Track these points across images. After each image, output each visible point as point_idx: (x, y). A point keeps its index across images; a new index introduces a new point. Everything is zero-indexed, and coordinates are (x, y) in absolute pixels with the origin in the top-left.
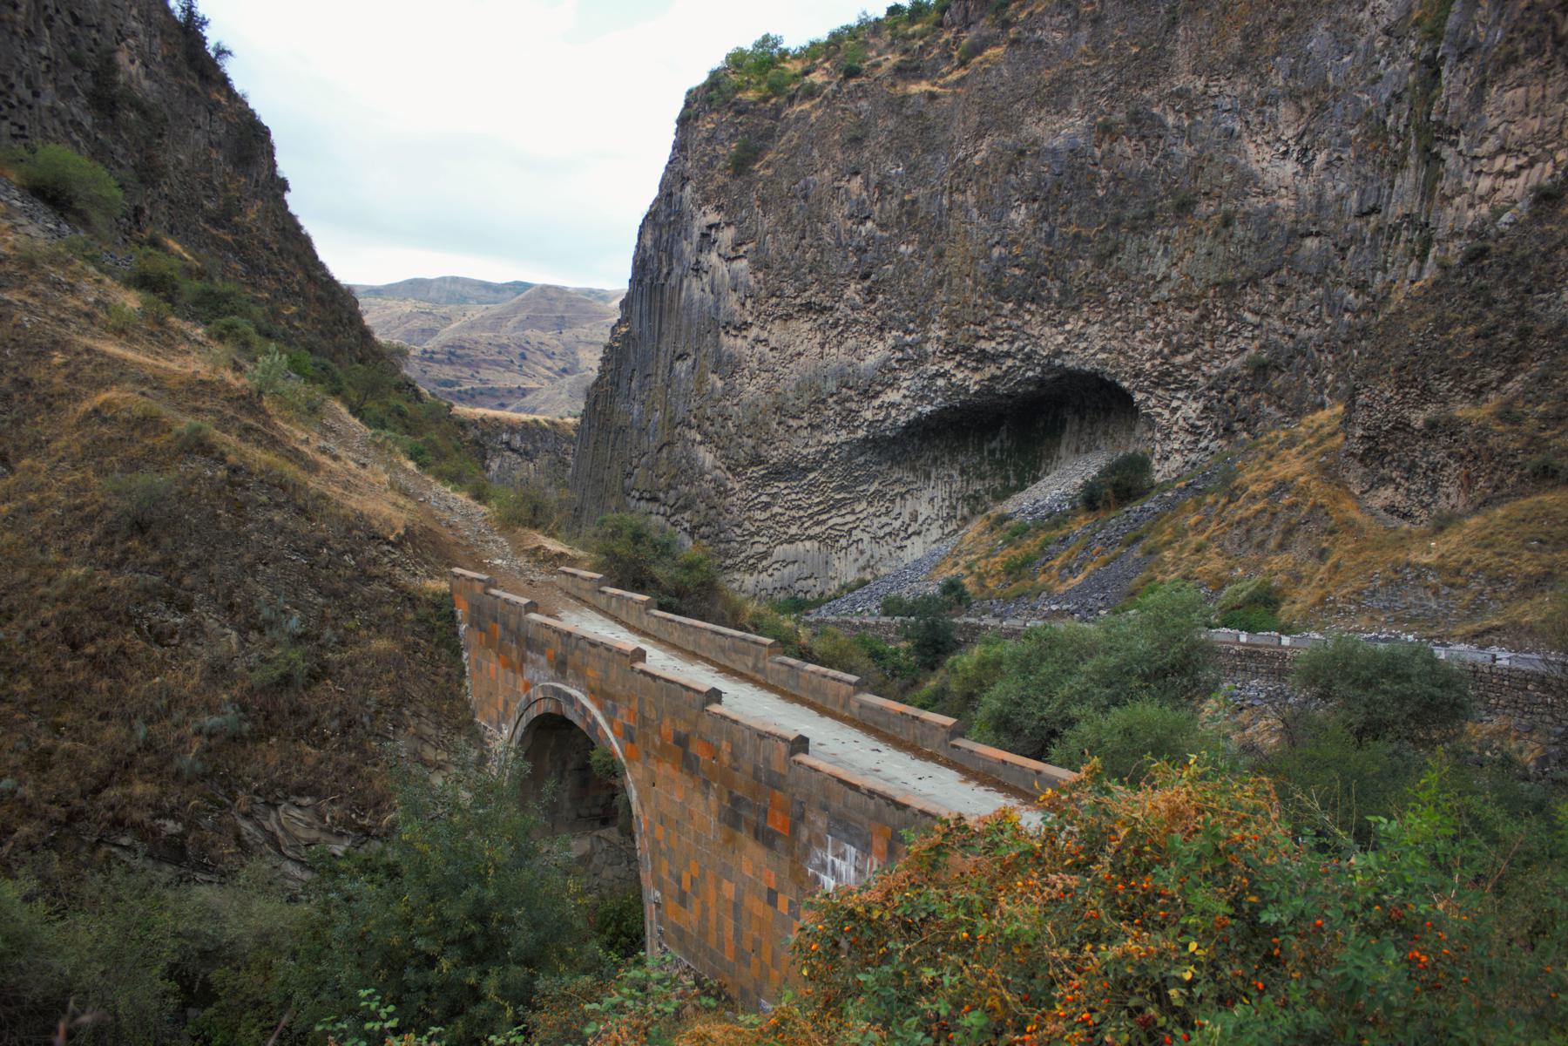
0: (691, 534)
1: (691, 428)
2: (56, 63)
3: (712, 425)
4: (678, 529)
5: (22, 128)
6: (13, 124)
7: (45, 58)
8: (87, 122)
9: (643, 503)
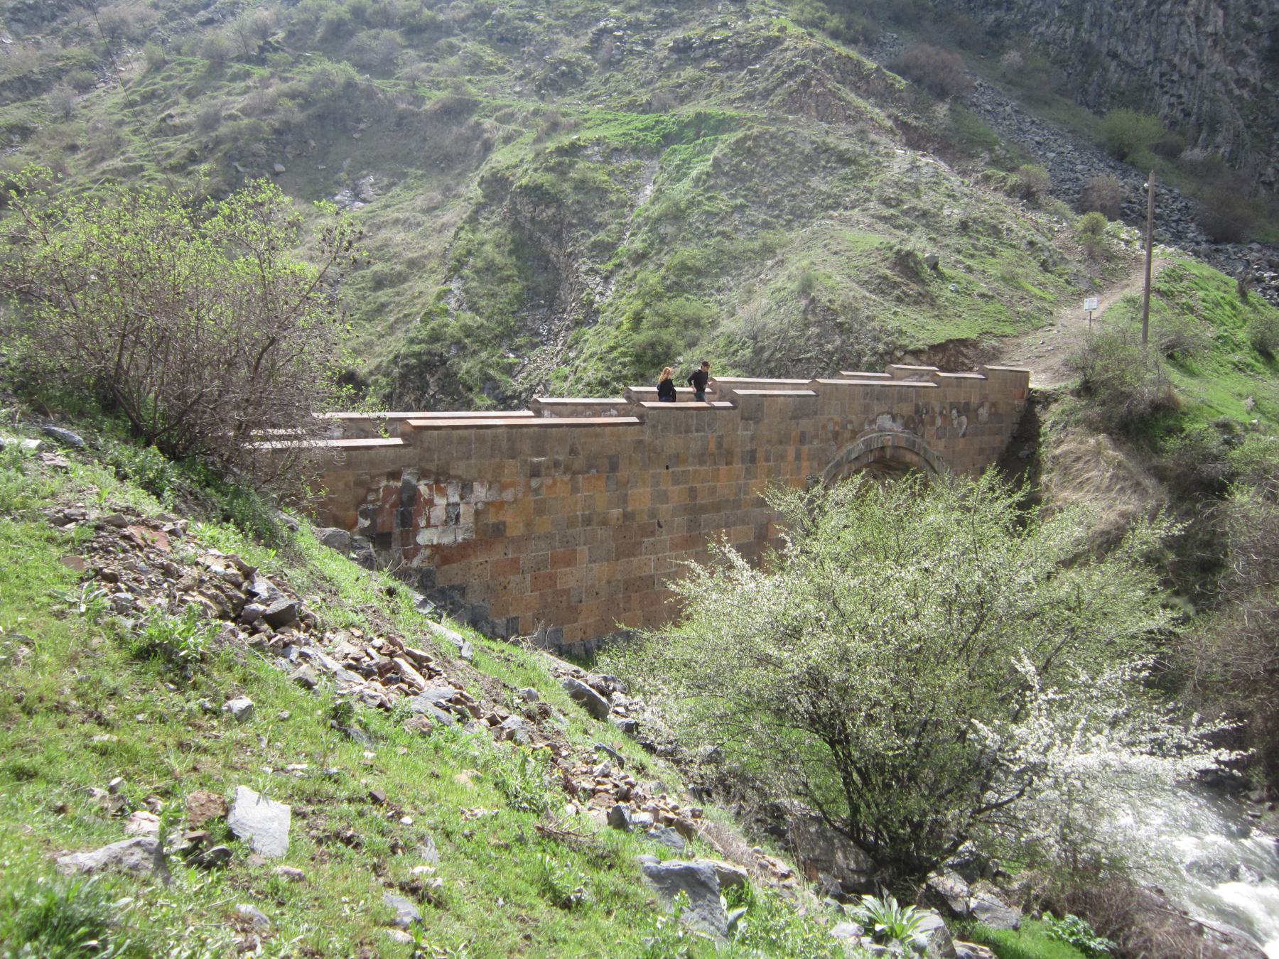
2: (1228, 36)
5: (1180, 97)
6: (1172, 95)
7: (1212, 34)
8: (1254, 77)
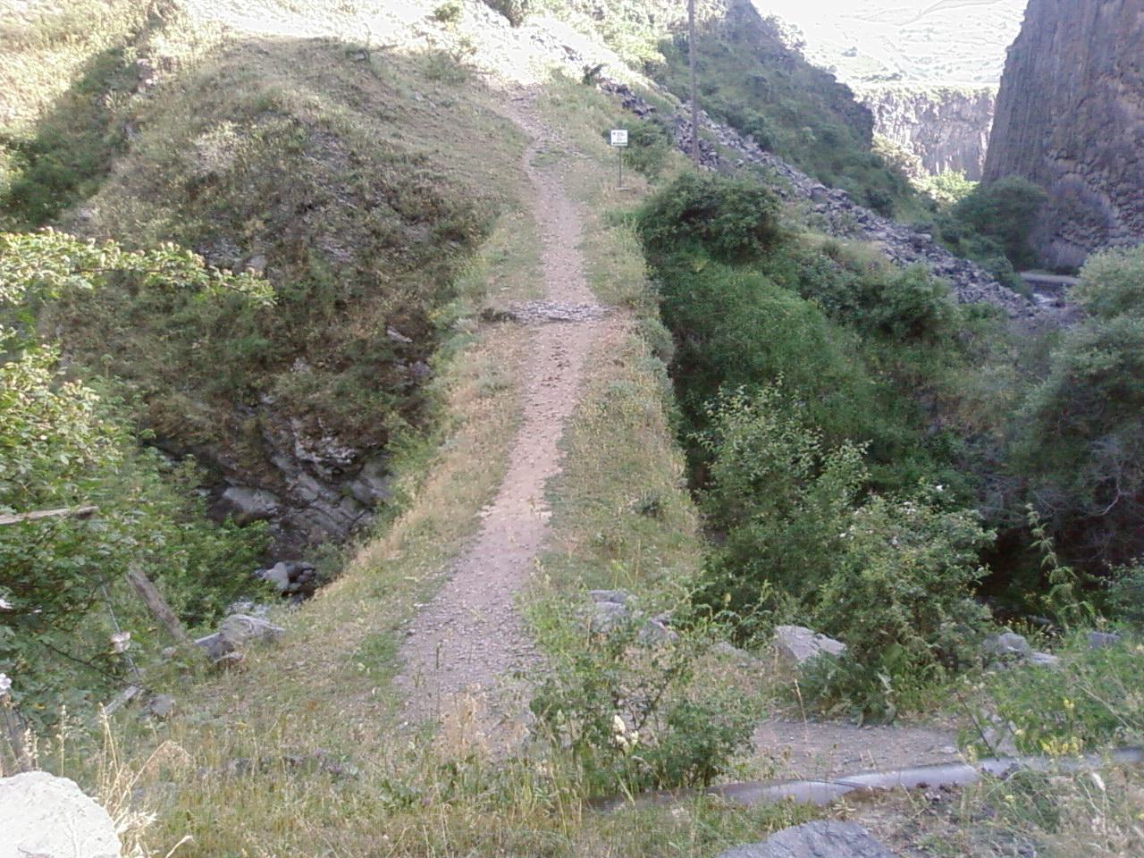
0: (1108, 191)
1: (1112, 74)
3: (1137, 71)
4: (1095, 187)
9: (1060, 162)
